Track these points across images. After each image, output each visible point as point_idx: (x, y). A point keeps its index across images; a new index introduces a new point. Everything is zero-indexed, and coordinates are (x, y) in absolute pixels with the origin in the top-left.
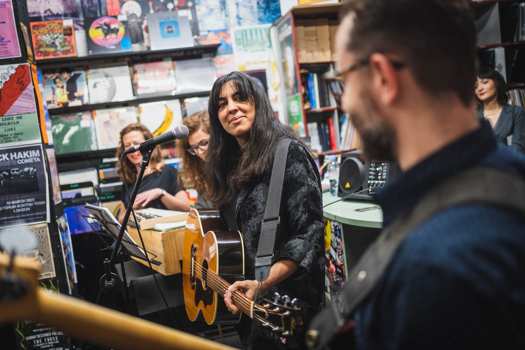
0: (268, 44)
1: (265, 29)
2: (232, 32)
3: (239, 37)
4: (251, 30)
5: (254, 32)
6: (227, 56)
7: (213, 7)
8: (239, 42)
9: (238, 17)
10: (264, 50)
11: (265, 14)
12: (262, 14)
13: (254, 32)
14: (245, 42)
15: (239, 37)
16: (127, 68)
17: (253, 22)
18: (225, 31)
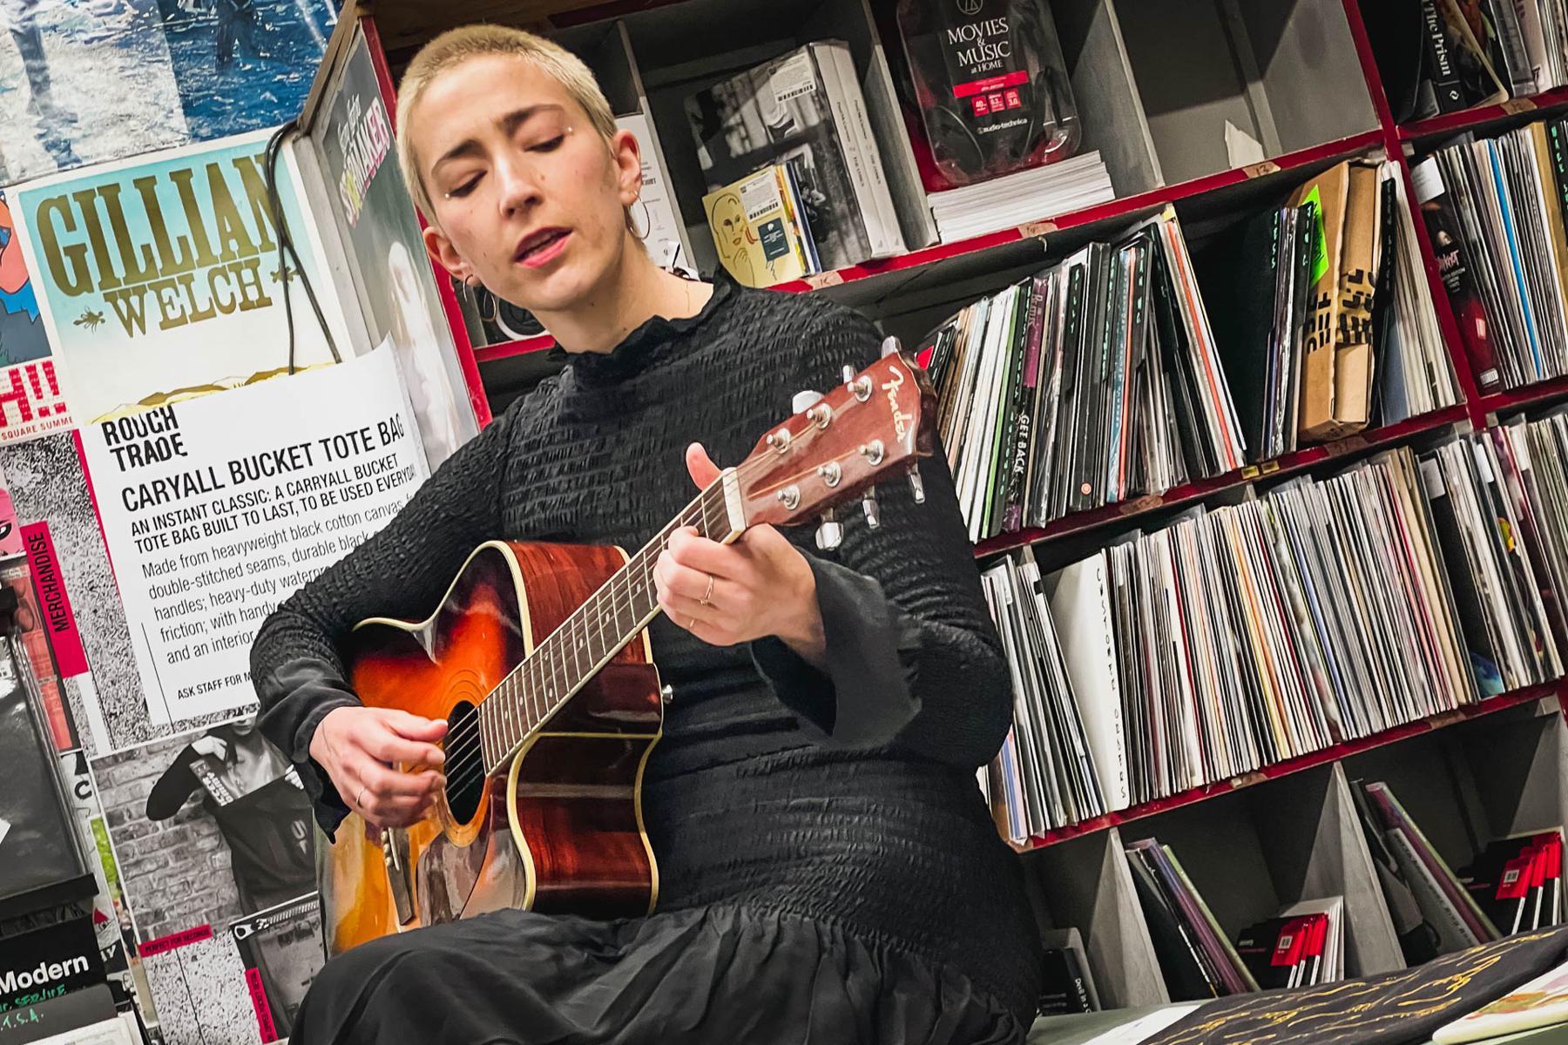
0: (270, 261)
5: (167, 193)
11: (224, 61)
13: (167, 193)
14: (119, 271)
15: (82, 236)
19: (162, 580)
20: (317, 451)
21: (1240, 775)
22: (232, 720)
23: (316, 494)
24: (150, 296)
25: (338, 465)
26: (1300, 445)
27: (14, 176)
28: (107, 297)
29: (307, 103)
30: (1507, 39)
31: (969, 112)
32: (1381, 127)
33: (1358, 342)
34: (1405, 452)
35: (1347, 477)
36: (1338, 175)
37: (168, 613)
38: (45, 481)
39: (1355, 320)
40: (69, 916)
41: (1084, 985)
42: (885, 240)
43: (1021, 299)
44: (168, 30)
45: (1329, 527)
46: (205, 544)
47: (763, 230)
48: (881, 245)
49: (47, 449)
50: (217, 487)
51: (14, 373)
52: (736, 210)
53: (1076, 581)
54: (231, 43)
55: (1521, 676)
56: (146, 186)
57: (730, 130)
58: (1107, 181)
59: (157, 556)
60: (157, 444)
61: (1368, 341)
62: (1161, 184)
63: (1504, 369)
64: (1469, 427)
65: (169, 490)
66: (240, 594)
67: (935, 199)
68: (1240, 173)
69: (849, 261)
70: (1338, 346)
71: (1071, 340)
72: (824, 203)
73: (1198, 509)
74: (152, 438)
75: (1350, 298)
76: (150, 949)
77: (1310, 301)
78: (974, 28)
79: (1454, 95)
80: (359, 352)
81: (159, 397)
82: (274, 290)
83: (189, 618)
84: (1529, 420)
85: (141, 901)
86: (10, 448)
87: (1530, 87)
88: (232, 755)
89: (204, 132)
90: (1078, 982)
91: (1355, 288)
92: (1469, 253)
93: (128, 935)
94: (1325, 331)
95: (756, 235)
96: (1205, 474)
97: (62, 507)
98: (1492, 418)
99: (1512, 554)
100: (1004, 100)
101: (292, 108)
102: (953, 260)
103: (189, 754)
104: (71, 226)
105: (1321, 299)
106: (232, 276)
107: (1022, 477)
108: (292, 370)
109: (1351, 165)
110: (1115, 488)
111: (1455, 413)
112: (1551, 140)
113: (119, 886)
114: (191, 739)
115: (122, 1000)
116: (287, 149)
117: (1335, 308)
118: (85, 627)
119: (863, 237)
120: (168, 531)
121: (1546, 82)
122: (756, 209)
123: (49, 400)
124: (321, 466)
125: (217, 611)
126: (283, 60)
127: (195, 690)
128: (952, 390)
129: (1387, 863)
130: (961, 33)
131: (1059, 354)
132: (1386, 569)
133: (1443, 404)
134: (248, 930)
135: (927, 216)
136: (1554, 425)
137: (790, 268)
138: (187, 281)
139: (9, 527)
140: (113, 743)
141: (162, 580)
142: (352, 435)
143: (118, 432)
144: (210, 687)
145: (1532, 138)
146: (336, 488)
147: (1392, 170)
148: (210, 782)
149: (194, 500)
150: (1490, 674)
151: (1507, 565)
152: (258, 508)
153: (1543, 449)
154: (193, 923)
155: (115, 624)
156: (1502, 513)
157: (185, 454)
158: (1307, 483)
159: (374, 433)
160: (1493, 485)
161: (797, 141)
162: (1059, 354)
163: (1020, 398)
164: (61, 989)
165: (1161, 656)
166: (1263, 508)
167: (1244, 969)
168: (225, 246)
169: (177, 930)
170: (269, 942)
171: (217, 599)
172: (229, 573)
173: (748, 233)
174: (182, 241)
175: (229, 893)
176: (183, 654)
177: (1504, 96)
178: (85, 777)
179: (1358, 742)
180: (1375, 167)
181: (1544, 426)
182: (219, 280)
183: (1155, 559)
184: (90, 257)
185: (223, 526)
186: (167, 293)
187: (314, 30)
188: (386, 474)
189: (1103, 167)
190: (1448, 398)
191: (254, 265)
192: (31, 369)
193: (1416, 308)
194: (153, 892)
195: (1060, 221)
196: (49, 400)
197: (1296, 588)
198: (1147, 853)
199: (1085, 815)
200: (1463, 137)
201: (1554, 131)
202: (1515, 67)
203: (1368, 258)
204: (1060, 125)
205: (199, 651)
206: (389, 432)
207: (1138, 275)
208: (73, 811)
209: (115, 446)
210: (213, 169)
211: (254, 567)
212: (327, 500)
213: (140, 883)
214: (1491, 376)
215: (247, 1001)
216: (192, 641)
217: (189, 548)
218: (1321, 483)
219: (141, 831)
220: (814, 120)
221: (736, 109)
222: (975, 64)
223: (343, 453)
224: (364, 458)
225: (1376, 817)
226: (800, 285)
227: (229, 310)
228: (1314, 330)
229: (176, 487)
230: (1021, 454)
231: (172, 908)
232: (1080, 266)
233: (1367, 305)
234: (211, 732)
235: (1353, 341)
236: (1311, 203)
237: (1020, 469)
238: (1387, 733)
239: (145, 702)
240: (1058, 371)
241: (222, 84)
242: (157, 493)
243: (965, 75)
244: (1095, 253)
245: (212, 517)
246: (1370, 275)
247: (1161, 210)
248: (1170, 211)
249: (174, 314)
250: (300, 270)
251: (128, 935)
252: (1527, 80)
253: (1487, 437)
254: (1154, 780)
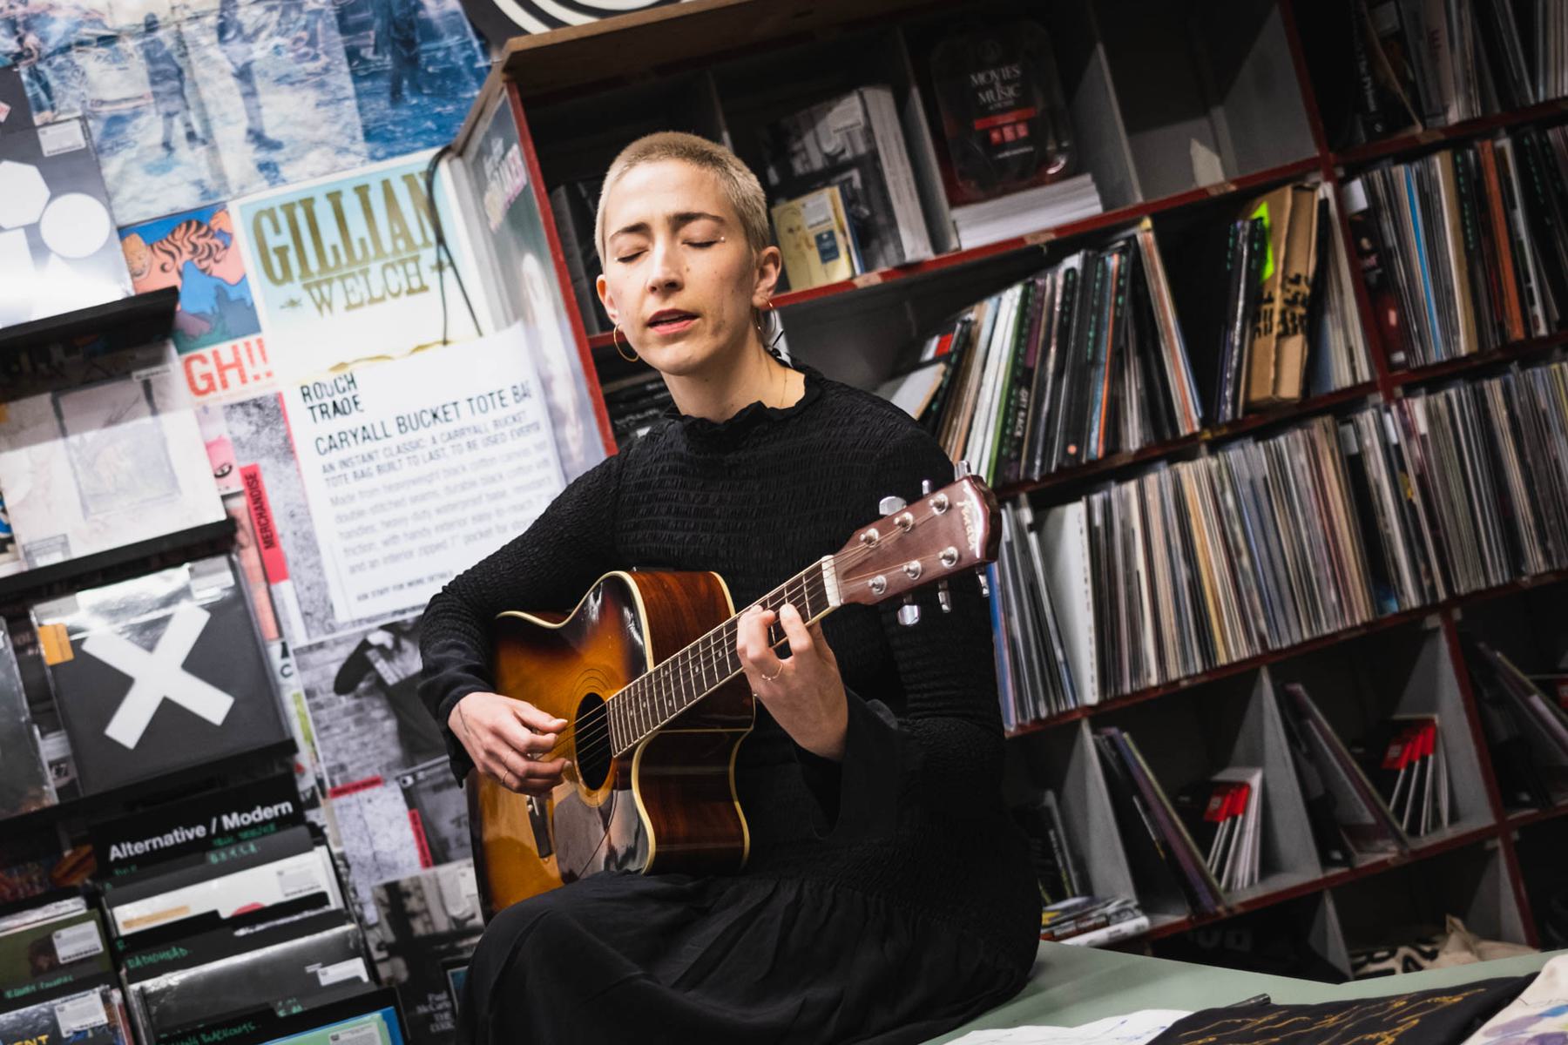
0: (429, 256)
1: (408, 179)
2: (237, 220)
5: (351, 204)
6: (225, 350)
7: (125, 108)
8: (276, 264)
9: (257, 137)
11: (396, 97)
12: (382, 104)
13: (351, 204)
15: (286, 238)
17: (342, 151)
19: (344, 509)
20: (464, 407)
21: (1188, 677)
22: (398, 618)
23: (463, 441)
24: (337, 285)
25: (479, 419)
26: (1246, 413)
27: (235, 191)
28: (307, 287)
29: (461, 129)
30: (1424, 81)
31: (986, 140)
32: (1317, 154)
33: (1295, 332)
34: (1328, 420)
35: (1282, 439)
36: (1283, 197)
37: (349, 535)
38: (258, 432)
39: (1293, 315)
40: (279, 770)
41: (1057, 835)
42: (914, 246)
43: (1025, 297)
44: (354, 73)
45: (1265, 479)
46: (377, 481)
47: (819, 238)
48: (913, 251)
49: (259, 406)
50: (386, 436)
51: (235, 348)
52: (796, 222)
53: (1060, 522)
54: (400, 82)
55: (1412, 599)
56: (335, 198)
57: (794, 154)
58: (1096, 198)
59: (342, 490)
60: (342, 403)
61: (1303, 331)
62: (1140, 199)
63: (1410, 352)
64: (1380, 398)
65: (351, 438)
66: (403, 520)
67: (958, 214)
68: (1203, 191)
69: (887, 264)
70: (1280, 336)
71: (1064, 330)
72: (868, 217)
73: (1162, 465)
74: (338, 398)
75: (1289, 296)
76: (337, 793)
77: (1257, 297)
78: (993, 74)
79: (1379, 128)
80: (497, 328)
81: (342, 365)
82: (431, 278)
83: (365, 539)
84: (1430, 392)
85: (329, 755)
86: (232, 406)
87: (1440, 122)
88: (397, 646)
89: (380, 153)
90: (1052, 833)
91: (1294, 288)
92: (1386, 257)
93: (320, 782)
94: (1268, 323)
95: (813, 241)
96: (1169, 436)
97: (270, 451)
98: (1399, 391)
99: (1410, 502)
100: (1015, 132)
101: (448, 133)
102: (968, 261)
103: (365, 645)
104: (277, 230)
105: (1266, 296)
106: (400, 269)
107: (1021, 440)
108: (445, 342)
109: (1295, 189)
110: (1096, 446)
111: (1370, 387)
112: (1455, 165)
113: (313, 745)
114: (367, 633)
115: (317, 836)
116: (443, 167)
117: (1278, 305)
118: (287, 544)
119: (899, 245)
120: (349, 471)
121: (1454, 115)
122: (813, 221)
123: (260, 368)
124: (466, 418)
125: (386, 533)
126: (441, 95)
127: (370, 595)
128: (967, 369)
129: (1299, 747)
130: (982, 78)
131: (1054, 341)
132: (1309, 513)
133: (1359, 380)
134: (410, 780)
135: (950, 226)
136: (1448, 400)
137: (841, 270)
138: (365, 272)
139: (230, 467)
140: (309, 636)
141: (344, 509)
142: (491, 394)
143: (312, 393)
144: (382, 592)
145: (1440, 165)
146: (478, 438)
147: (1326, 190)
148: (381, 666)
149: (369, 446)
150: (1387, 597)
151: (1404, 507)
152: (418, 452)
153: (1439, 417)
154: (368, 775)
155: (309, 543)
156: (1403, 468)
157: (362, 411)
158: (1250, 446)
159: (508, 394)
160: (1398, 447)
161: (849, 165)
162: (1054, 341)
163: (1021, 375)
164: (272, 827)
165: (1128, 582)
166: (1213, 463)
167: (1180, 824)
168: (395, 244)
169: (357, 779)
170: (425, 790)
171: (388, 524)
172: (397, 504)
173: (807, 240)
174: (362, 241)
175: (395, 752)
176: (360, 567)
177: (1419, 129)
178: (287, 661)
179: (1281, 651)
180: (1313, 190)
181: (1440, 400)
182: (389, 272)
183: (1125, 503)
184: (292, 256)
185: (391, 466)
186: (350, 282)
187: (465, 70)
188: (517, 426)
189: (1093, 187)
190: (1364, 374)
191: (416, 259)
192: (247, 344)
193: (1342, 301)
194: (338, 750)
195: (1058, 230)
196: (260, 368)
197: (1237, 529)
198: (1111, 739)
199: (1063, 708)
200: (1384, 163)
201: (1459, 159)
202: (1429, 104)
203: (1306, 265)
204: (1060, 151)
205: (373, 564)
206: (521, 394)
207: (1119, 276)
208: (278, 687)
209: (310, 404)
210: (386, 184)
211: (414, 500)
212: (471, 445)
213: (329, 743)
214: (1400, 357)
215: (409, 834)
216: (366, 557)
217: (365, 484)
218: (1261, 445)
219: (330, 703)
220: (862, 149)
221: (800, 137)
222: (993, 103)
223: (483, 408)
224: (500, 413)
225: (1292, 712)
226: (848, 284)
227: (396, 295)
228: (1259, 321)
229: (355, 436)
230: (1020, 421)
231: (352, 763)
232: (1072, 270)
233: (1303, 304)
234: (384, 628)
235: (1291, 331)
236: (1261, 219)
237: (1019, 434)
238: (1304, 643)
239: (332, 607)
240: (1053, 350)
241: (395, 115)
242: (341, 441)
243: (985, 111)
244: (1086, 261)
245: (382, 460)
246: (1306, 278)
247: (1137, 222)
248: (1147, 223)
249: (354, 300)
250: (452, 264)
251: (320, 782)
252: (1438, 115)
253: (1394, 408)
254: (1118, 679)
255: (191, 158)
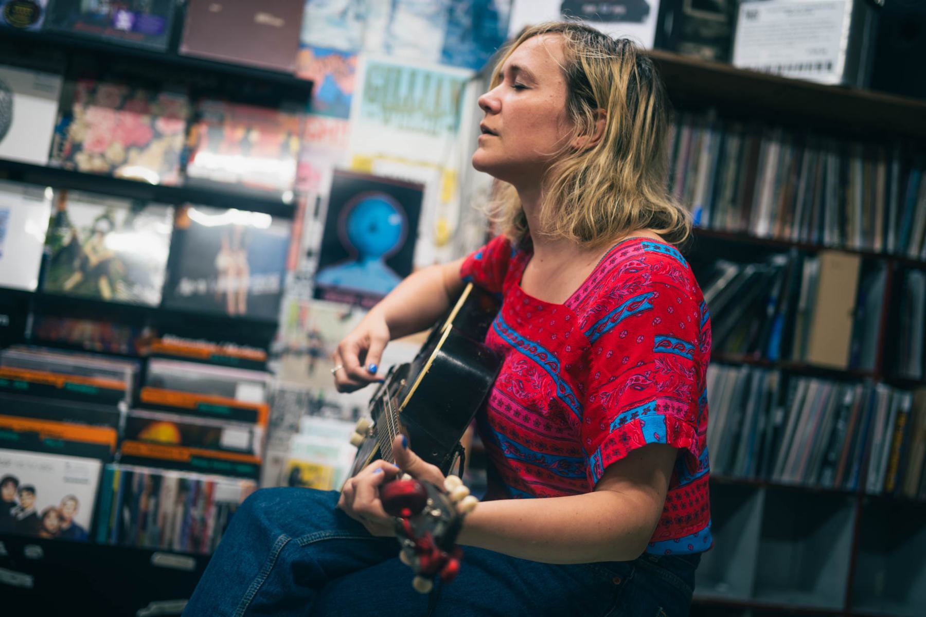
2: (361, 64)
3: (378, 81)
4: (413, 74)
8: (372, 94)
10: (434, 133)
12: (454, 41)
16: (56, 82)
18: (344, 56)
255: (354, 29)
